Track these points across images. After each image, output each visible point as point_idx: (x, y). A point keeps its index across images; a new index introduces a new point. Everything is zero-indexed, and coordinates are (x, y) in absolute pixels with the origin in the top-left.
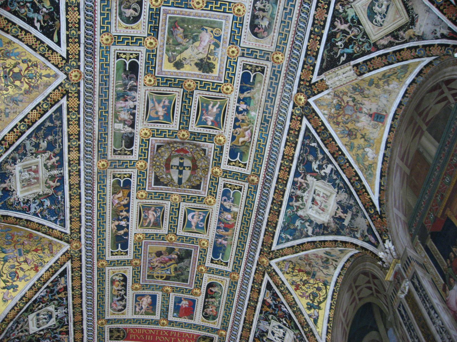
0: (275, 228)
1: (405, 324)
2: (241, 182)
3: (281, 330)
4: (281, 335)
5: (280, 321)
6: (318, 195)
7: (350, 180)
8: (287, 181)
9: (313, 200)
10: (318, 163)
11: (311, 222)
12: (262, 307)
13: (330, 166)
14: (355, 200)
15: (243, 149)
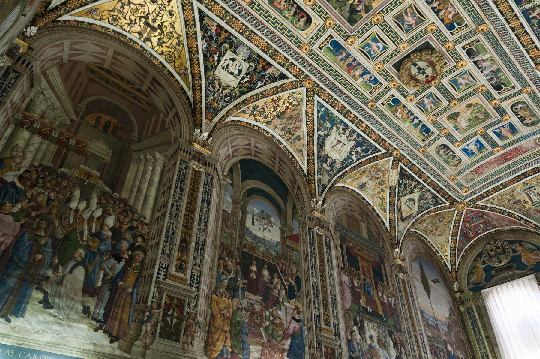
0: (331, 105)
1: (310, 239)
2: (375, 95)
3: (236, 72)
4: (231, 69)
5: (247, 74)
6: (342, 147)
7: (346, 172)
8: (358, 127)
9: (340, 142)
10: (360, 152)
11: (327, 136)
12: (265, 60)
13: (355, 159)
14: (336, 174)
15: (394, 108)
